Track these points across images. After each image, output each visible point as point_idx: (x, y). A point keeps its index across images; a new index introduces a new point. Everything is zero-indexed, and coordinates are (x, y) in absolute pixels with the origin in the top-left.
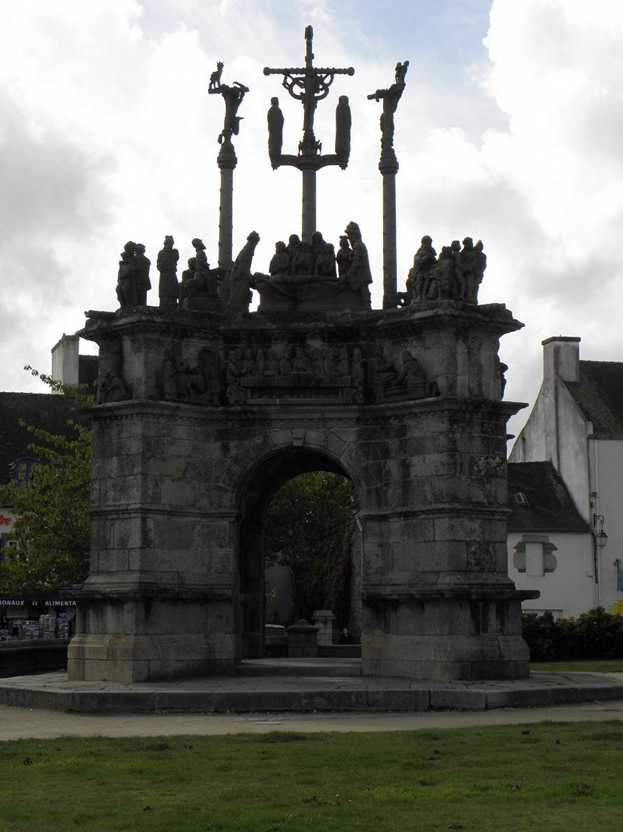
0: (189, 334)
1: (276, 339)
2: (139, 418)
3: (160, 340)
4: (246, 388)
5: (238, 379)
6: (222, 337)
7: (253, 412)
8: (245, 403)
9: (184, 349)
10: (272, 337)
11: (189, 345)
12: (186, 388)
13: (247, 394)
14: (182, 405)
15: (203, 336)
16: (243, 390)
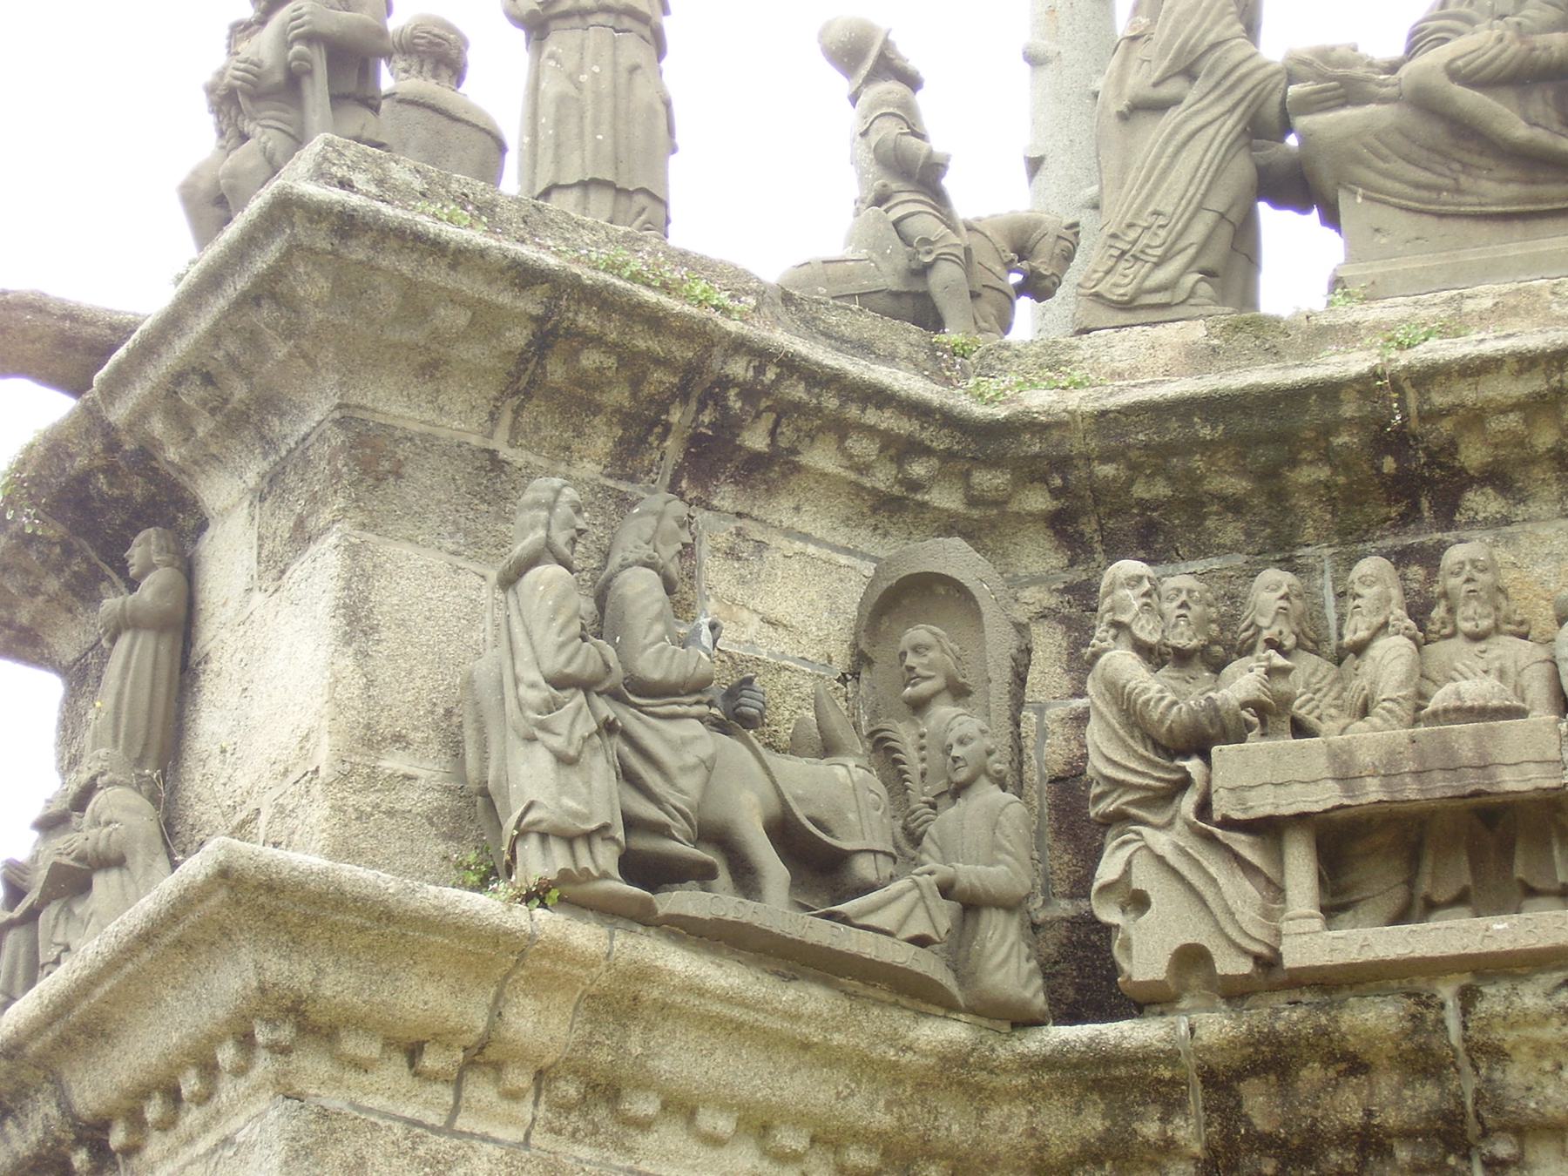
0: (756, 440)
1: (1498, 478)
2: (264, 1065)
3: (495, 463)
4: (1269, 830)
5: (1193, 766)
6: (1038, 501)
7: (1355, 1065)
8: (1268, 963)
9: (716, 574)
10: (1473, 455)
11: (761, 546)
12: (719, 837)
13: (1276, 890)
14: (678, 961)
15: (883, 478)
16: (1242, 844)
